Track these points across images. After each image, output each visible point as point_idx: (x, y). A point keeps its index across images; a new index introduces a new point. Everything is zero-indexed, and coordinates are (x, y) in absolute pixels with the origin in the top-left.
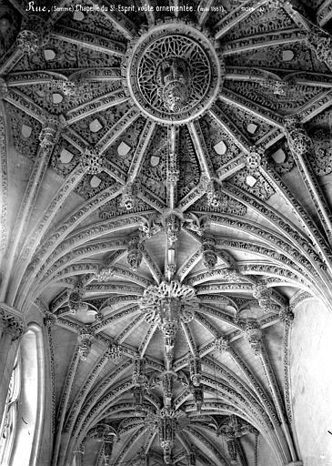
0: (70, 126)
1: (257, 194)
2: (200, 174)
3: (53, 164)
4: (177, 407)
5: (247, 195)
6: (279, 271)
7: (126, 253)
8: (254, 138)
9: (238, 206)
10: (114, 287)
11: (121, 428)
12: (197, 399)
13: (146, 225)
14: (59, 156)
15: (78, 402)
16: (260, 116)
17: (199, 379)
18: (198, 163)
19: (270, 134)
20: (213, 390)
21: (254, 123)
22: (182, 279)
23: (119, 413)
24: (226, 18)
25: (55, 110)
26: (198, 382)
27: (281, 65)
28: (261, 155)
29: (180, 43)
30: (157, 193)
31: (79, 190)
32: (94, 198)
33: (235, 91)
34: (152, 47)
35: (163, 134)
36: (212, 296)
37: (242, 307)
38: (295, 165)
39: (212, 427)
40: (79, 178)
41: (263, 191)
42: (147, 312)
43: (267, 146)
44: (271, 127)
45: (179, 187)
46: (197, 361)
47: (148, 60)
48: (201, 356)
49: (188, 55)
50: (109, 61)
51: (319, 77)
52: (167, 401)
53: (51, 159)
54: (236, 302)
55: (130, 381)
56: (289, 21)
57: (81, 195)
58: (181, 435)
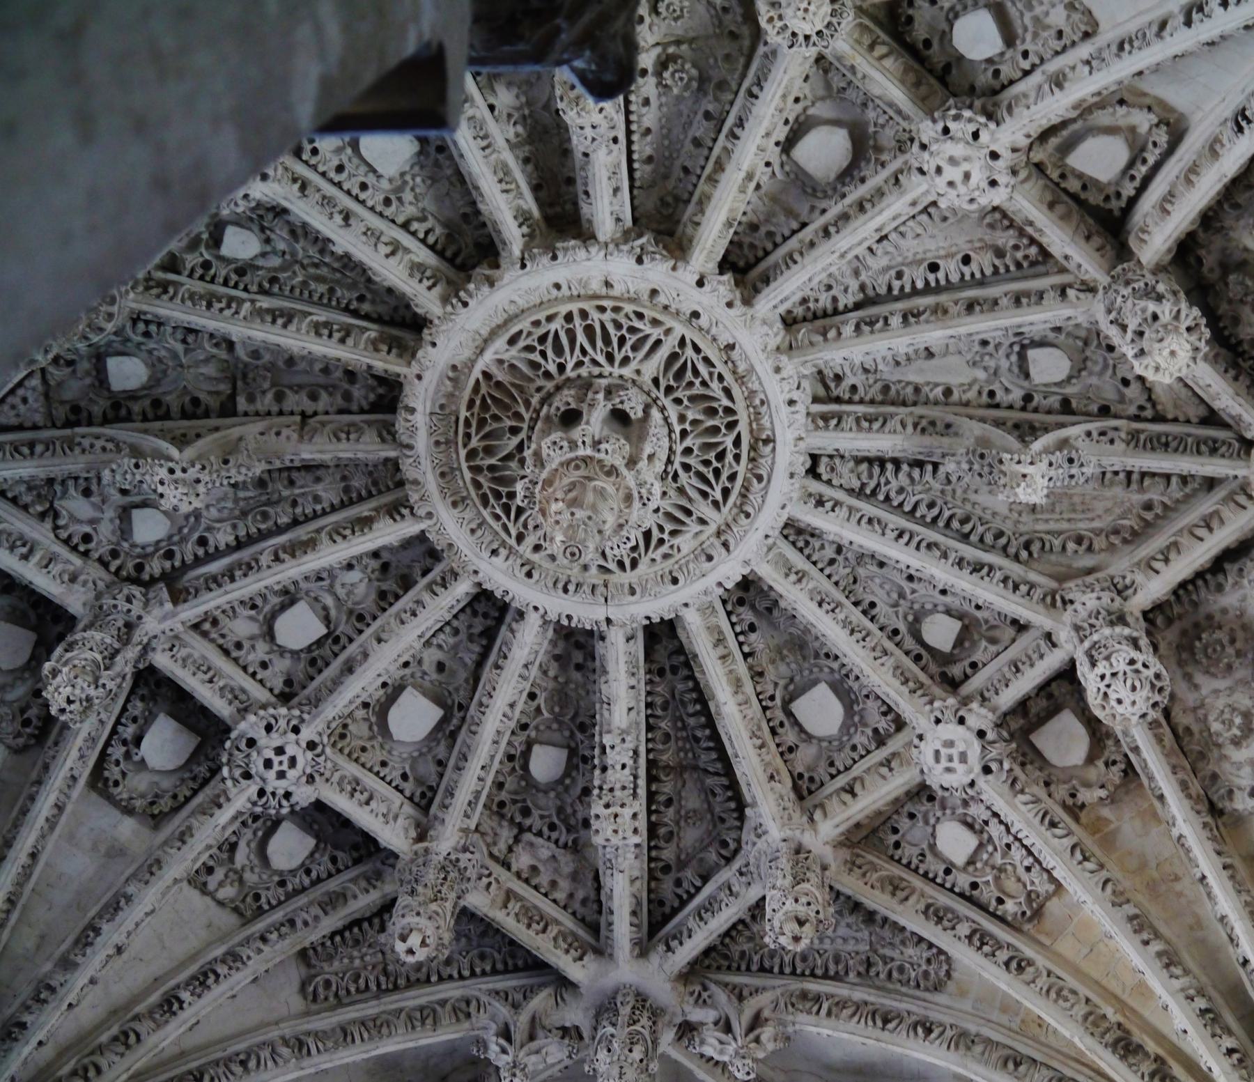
0: (196, 627)
1: (988, 894)
2: (742, 818)
5: (944, 899)
8: (956, 671)
9: (910, 951)
13: (506, 1034)
16: (966, 585)
18: (729, 771)
19: (1013, 652)
21: (948, 612)
24: (793, 243)
25: (139, 568)
27: (1028, 398)
28: (981, 734)
29: (618, 326)
30: (560, 896)
31: (213, 881)
32: (278, 915)
33: (859, 493)
34: (512, 341)
35: (578, 657)
38: (1129, 771)
41: (1010, 885)
43: (1008, 698)
44: (1020, 627)
45: (656, 871)
47: (499, 385)
49: (653, 367)
50: (357, 392)
51: (1181, 439)
56: (1033, 251)
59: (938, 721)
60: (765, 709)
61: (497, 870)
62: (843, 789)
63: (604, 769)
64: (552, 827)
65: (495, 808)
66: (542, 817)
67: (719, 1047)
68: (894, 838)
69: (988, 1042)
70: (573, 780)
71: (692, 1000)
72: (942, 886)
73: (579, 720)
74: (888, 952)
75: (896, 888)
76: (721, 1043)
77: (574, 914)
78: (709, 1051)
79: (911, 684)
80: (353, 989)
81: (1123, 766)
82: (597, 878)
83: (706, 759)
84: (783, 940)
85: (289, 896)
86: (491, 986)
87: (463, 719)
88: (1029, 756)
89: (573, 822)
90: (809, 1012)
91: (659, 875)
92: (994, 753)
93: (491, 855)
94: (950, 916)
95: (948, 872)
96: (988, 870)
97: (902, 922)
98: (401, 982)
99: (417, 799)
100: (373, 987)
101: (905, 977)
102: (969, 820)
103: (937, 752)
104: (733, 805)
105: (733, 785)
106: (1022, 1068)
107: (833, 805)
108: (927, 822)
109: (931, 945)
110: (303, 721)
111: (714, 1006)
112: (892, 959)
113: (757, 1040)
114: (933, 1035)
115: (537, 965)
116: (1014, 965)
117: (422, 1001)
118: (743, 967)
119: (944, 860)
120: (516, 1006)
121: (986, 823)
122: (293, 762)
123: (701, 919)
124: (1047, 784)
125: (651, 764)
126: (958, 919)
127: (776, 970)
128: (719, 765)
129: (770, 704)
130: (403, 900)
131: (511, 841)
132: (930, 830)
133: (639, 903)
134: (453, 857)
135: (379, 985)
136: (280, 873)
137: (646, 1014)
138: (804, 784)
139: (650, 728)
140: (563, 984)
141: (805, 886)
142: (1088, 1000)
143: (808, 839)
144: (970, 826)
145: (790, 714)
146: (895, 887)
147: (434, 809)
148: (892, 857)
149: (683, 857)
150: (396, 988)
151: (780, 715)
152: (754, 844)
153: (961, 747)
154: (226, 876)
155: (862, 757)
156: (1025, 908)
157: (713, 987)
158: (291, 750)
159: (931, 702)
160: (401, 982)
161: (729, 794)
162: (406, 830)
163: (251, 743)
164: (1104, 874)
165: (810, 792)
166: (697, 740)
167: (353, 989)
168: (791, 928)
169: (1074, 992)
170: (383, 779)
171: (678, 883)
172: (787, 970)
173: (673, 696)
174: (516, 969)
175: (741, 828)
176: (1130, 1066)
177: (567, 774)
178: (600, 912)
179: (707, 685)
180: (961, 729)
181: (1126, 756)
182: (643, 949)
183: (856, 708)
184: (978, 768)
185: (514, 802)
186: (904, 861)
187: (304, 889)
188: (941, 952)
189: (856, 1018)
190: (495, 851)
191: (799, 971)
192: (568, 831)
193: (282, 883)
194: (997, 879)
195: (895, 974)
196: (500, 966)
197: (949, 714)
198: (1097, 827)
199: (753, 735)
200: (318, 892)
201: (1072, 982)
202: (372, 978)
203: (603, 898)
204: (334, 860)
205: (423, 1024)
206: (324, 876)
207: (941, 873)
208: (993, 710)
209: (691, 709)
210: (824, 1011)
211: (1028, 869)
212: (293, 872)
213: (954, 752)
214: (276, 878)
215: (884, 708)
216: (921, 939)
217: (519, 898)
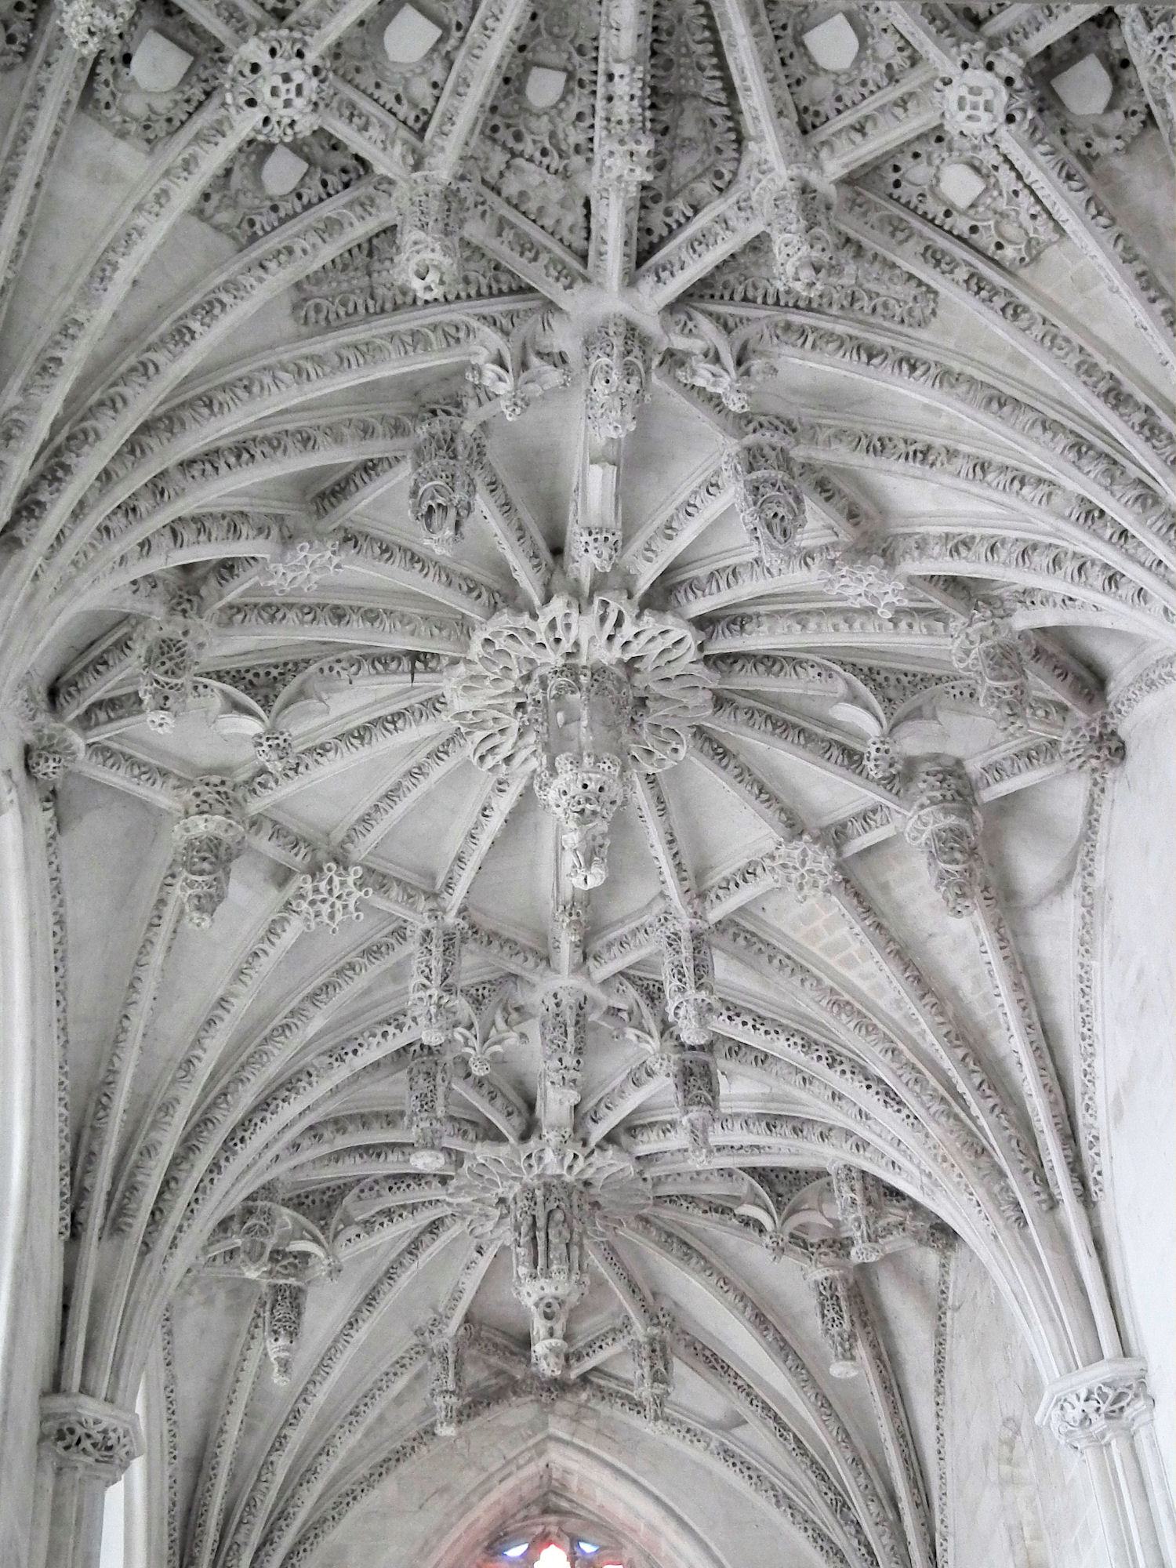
1: (986, 240)
3: (103, 94)
4: (598, 1132)
5: (942, 242)
6: (1070, 566)
7: (404, 473)
10: (339, 615)
11: (348, 1222)
12: (689, 1101)
14: (127, 59)
15: (167, 1108)
17: (705, 1011)
20: (763, 1059)
22: (643, 585)
23: (337, 1156)
26: (703, 1023)
28: (1009, 81)
32: (273, 242)
36: (767, 661)
37: (901, 709)
39: (747, 1222)
40: (214, 159)
41: (1010, 230)
42: (480, 726)
43: (1036, 44)
46: (697, 936)
48: (715, 914)
52: (555, 1105)
53: (93, 74)
54: (878, 688)
55: (396, 1020)
57: (217, 228)
58: (611, 1253)
59: (965, 66)
60: (777, 37)
61: (490, 196)
62: (853, 128)
63: (610, 99)
64: (544, 153)
65: (488, 132)
66: (534, 142)
67: (712, 379)
68: (896, 176)
69: (971, 380)
70: (568, 104)
71: (678, 329)
72: (941, 227)
73: (577, 43)
74: (872, 286)
75: (896, 229)
76: (714, 375)
77: (561, 240)
78: (700, 382)
79: (938, 22)
80: (342, 313)
81: (1143, 117)
82: (587, 204)
83: (712, 88)
84: (798, 286)
85: (282, 221)
86: (478, 311)
87: (462, 39)
88: (1048, 103)
89: (564, 147)
90: (794, 346)
91: (649, 203)
92: (1020, 102)
93: (484, 181)
94: (947, 259)
95: (948, 214)
96: (990, 214)
97: (899, 262)
98: (388, 306)
99: (411, 122)
100: (361, 310)
101: (890, 313)
102: (977, 163)
103: (961, 100)
104: (733, 136)
105: (734, 115)
106: (1007, 409)
107: (841, 144)
108: (930, 163)
109: (920, 283)
110: (305, 44)
111: (701, 338)
112: (878, 295)
113: (747, 373)
114: (918, 373)
115: (526, 290)
116: (1010, 311)
117: (414, 325)
118: (727, 297)
119: (945, 203)
120: (506, 333)
121: (996, 168)
122: (299, 90)
123: (695, 251)
124: (1063, 132)
125: (654, 90)
126: (954, 264)
127: (760, 300)
128: (722, 97)
129: (781, 33)
130: (409, 236)
131: (503, 167)
132: (933, 171)
133: (630, 232)
134: (454, 187)
135: (367, 309)
136: (271, 199)
137: (637, 343)
138: (809, 119)
139: (654, 53)
140: (551, 306)
141: (817, 230)
142: (1081, 349)
143: (813, 178)
144: (977, 170)
145: (801, 44)
146: (896, 227)
147: (429, 134)
148: (891, 196)
149: (673, 186)
150: (383, 310)
151: (791, 46)
152: (759, 181)
153: (988, 94)
154: (221, 201)
155: (872, 92)
156: (1024, 254)
157: (700, 318)
158: (298, 77)
159: (958, 45)
160: (388, 306)
161: (731, 124)
162: (404, 157)
163: (255, 68)
164: (1116, 230)
165: (814, 127)
166: (702, 69)
167: (342, 313)
168: (807, 274)
169: (1067, 340)
170: (376, 101)
171: (668, 213)
172: (770, 301)
173: (680, 20)
174: (501, 293)
175: (739, 160)
176: (1121, 415)
177: (563, 99)
178: (588, 239)
179: (723, 15)
180: (989, 76)
181: (1148, 106)
182: (631, 280)
183: (870, 41)
184: (1002, 118)
185: (508, 126)
186: (903, 200)
187: (296, 214)
188: (930, 290)
189: (841, 353)
190: (487, 177)
191: (782, 303)
192: (561, 157)
193: (275, 208)
194: (997, 224)
195: (880, 310)
196: (485, 290)
197: (976, 60)
198: (1107, 179)
199: (767, 70)
200: (310, 218)
201: (1065, 330)
202: (360, 302)
203: (593, 226)
204: (324, 184)
205: (415, 349)
206: (315, 200)
207: (941, 215)
208: (1022, 55)
209: (698, 37)
210: (809, 344)
211: (1034, 217)
212: (283, 197)
213: (981, 100)
214: (268, 203)
215: (901, 44)
216: (911, 277)
217: (513, 226)
